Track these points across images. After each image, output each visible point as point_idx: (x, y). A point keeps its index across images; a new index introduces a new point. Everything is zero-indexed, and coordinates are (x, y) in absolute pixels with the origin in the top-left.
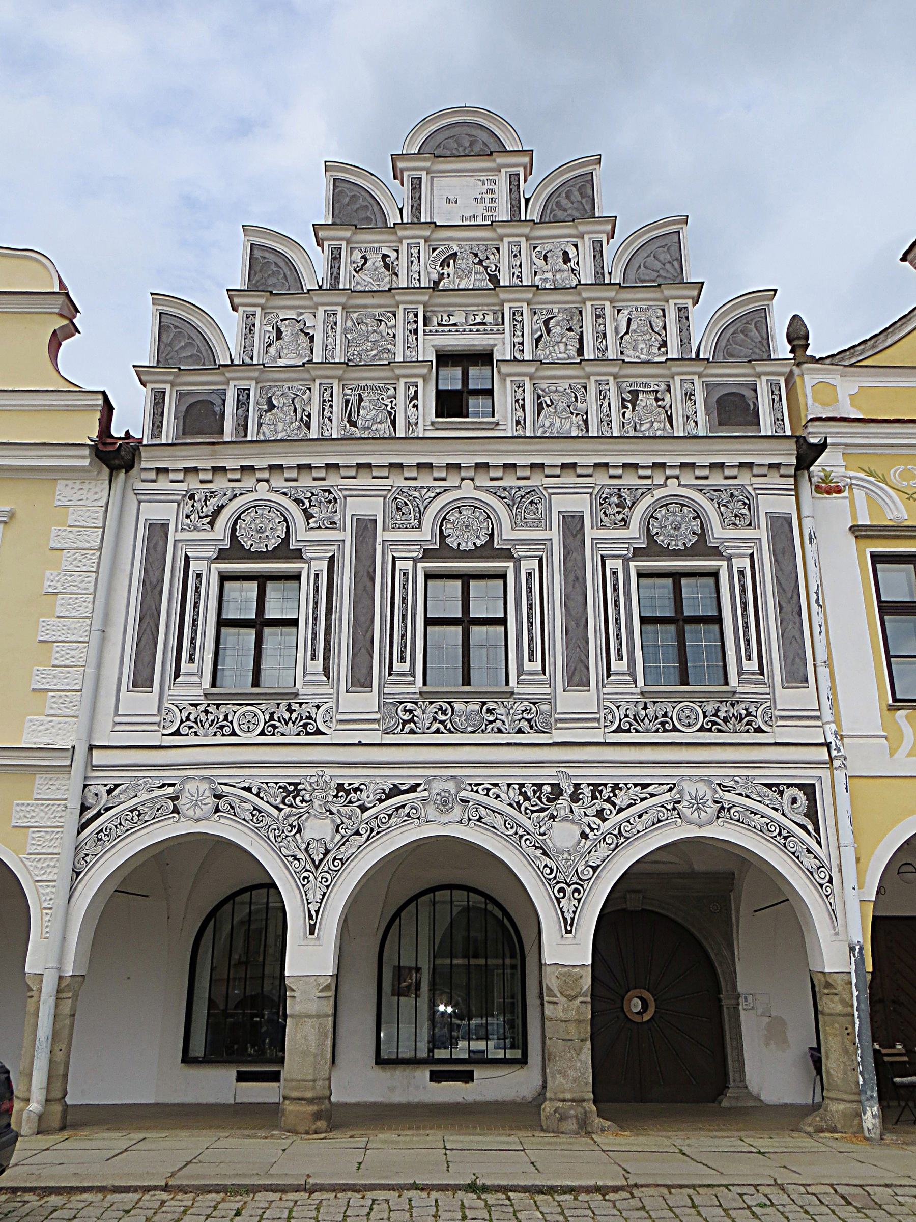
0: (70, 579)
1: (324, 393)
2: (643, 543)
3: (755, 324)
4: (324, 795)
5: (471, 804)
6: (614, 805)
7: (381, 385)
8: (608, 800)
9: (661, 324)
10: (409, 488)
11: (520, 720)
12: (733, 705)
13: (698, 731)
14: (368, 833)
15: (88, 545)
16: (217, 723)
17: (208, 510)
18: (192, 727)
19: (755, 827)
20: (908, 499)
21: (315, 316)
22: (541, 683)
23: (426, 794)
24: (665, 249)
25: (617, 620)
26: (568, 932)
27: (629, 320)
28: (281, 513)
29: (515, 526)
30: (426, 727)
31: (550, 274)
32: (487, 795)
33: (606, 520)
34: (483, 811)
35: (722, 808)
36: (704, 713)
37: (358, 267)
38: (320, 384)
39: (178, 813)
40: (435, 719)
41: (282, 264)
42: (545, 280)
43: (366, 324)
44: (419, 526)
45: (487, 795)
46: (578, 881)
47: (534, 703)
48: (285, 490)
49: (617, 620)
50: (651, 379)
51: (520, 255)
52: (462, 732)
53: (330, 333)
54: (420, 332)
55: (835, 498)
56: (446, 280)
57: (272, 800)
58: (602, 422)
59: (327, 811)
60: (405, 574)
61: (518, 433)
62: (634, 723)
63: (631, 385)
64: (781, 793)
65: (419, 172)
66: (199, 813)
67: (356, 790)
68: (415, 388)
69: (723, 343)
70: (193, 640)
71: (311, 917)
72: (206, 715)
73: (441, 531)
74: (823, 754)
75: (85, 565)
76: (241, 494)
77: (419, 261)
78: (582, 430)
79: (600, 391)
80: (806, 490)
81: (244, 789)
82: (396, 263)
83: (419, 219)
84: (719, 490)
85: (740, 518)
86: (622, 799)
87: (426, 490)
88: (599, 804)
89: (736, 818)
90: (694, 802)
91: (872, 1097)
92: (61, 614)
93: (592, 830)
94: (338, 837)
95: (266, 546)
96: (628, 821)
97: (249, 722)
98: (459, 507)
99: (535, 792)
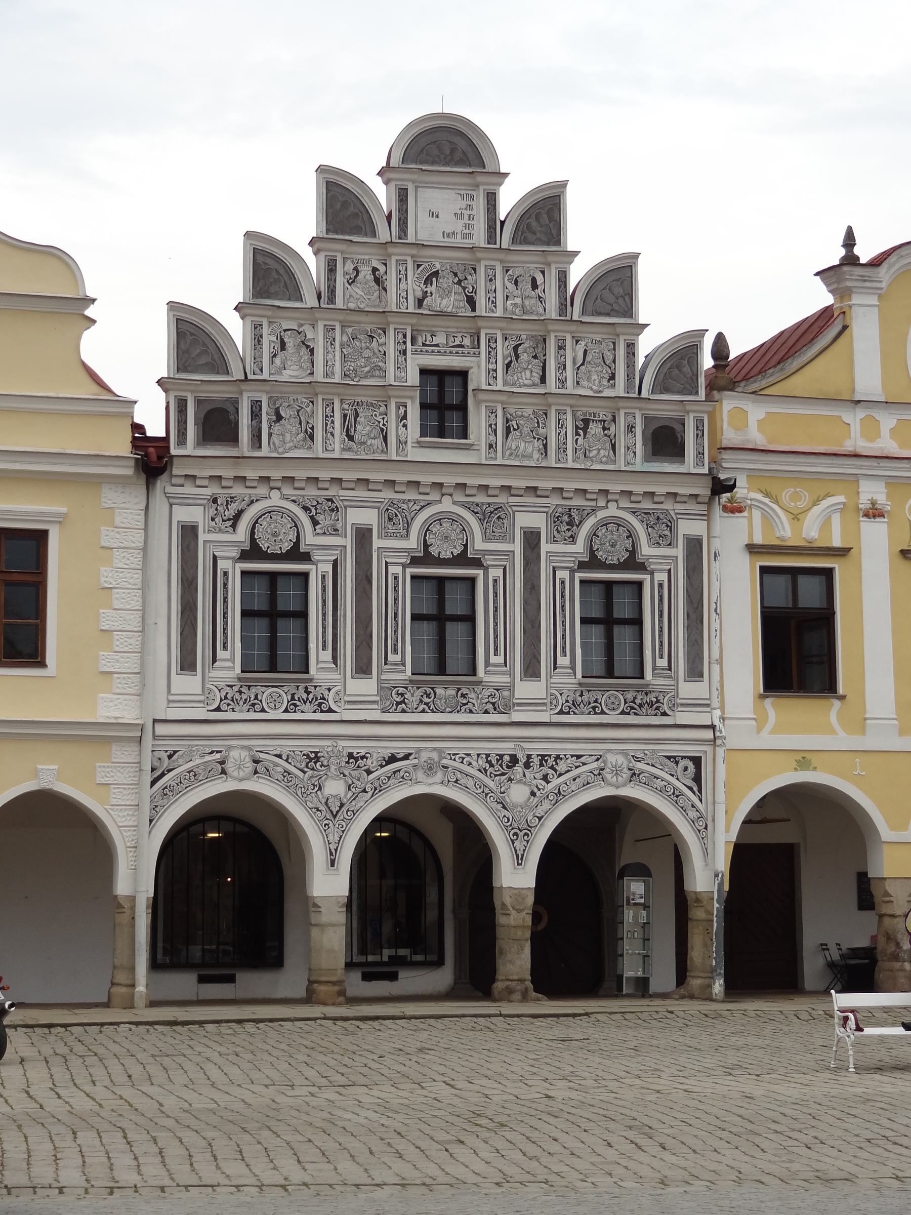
0: (121, 575)
1: (326, 408)
2: (586, 557)
3: (688, 361)
4: (339, 761)
5: (449, 769)
6: (556, 771)
7: (374, 402)
8: (552, 768)
9: (611, 357)
10: (399, 501)
11: (486, 703)
12: (647, 694)
13: (621, 713)
14: (373, 791)
15: (134, 545)
16: (250, 701)
17: (230, 514)
18: (230, 705)
19: (656, 789)
20: (793, 519)
21: (314, 328)
22: (503, 673)
23: (416, 761)
24: (619, 283)
25: (563, 623)
26: (519, 864)
27: (585, 352)
28: (292, 519)
29: (486, 538)
30: (414, 708)
31: (520, 299)
32: (462, 762)
33: (558, 536)
34: (459, 775)
35: (634, 774)
36: (625, 700)
37: (350, 279)
38: (323, 399)
39: (226, 774)
40: (421, 701)
41: (282, 271)
42: (515, 305)
43: (359, 339)
44: (407, 535)
45: (462, 762)
46: (528, 828)
47: (498, 690)
48: (294, 498)
49: (563, 623)
50: (599, 410)
51: (495, 279)
52: (442, 712)
53: (330, 349)
54: (409, 353)
55: (737, 517)
56: (429, 299)
57: (298, 765)
58: (559, 449)
59: (341, 773)
60: (396, 578)
61: (490, 455)
62: (572, 707)
63: (584, 414)
64: (677, 763)
65: (406, 183)
66: (242, 774)
67: (363, 757)
68: (404, 409)
69: (661, 377)
70: (225, 629)
71: (331, 854)
72: (240, 694)
73: (425, 540)
74: (709, 734)
75: (133, 563)
76: (257, 500)
77: (406, 280)
78: (542, 454)
79: (559, 420)
80: (717, 511)
81: (276, 756)
82: (384, 278)
83: (406, 235)
84: (648, 513)
85: (663, 538)
86: (562, 767)
87: (413, 503)
88: (545, 770)
89: (644, 781)
90: (614, 769)
91: (720, 973)
92: (117, 607)
93: (539, 789)
94: (350, 794)
95: (281, 548)
96: (566, 784)
97: (275, 701)
98: (439, 520)
99: (498, 760)
